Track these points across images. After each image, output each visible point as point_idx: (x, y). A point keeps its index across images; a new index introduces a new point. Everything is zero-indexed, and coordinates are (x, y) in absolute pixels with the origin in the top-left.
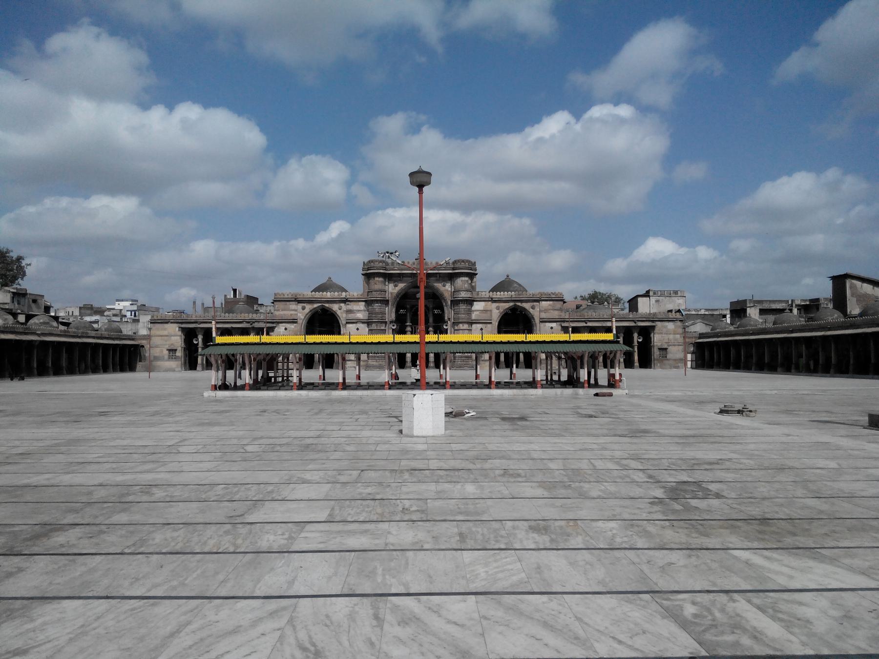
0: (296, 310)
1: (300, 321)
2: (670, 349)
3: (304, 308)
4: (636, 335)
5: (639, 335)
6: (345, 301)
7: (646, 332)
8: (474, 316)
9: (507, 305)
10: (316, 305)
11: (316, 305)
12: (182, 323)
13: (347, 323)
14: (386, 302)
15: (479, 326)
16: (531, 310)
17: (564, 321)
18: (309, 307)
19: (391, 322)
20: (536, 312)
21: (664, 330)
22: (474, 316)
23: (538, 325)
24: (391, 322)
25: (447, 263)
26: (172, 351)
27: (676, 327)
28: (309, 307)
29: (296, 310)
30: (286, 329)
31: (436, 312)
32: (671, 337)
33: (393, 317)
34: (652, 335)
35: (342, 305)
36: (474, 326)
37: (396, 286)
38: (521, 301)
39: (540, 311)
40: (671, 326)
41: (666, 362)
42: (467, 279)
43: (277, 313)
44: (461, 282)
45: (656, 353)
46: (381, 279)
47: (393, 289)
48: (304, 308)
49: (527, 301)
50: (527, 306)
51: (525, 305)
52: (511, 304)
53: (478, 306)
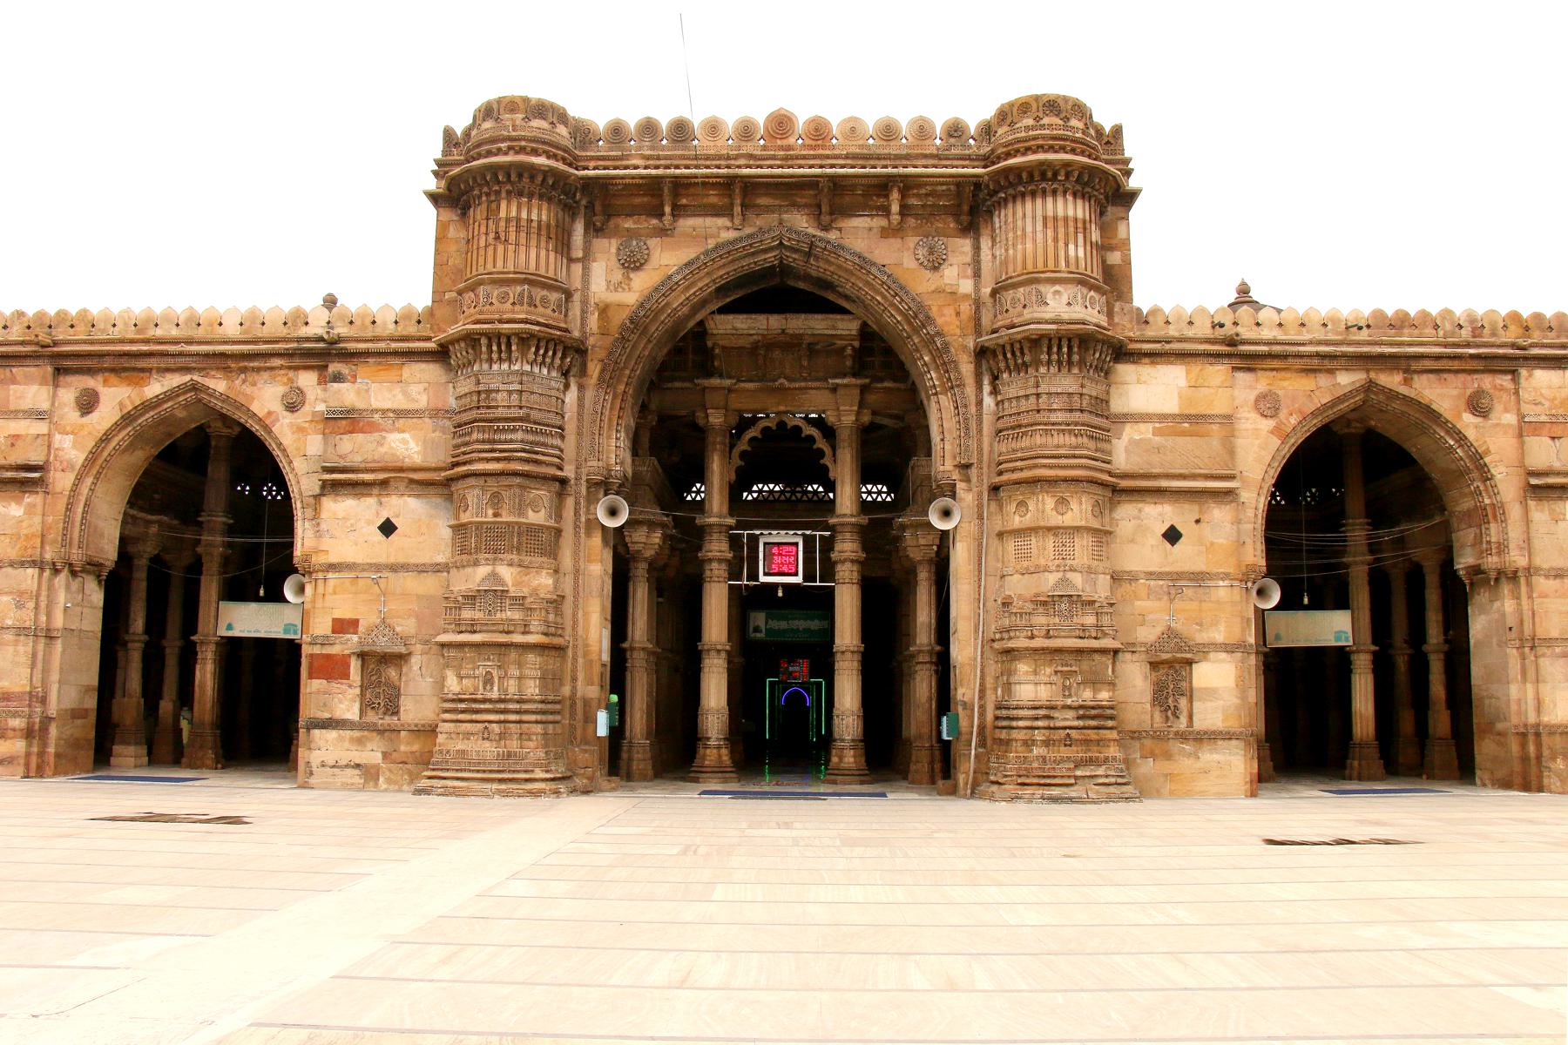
0: (39, 415)
1: (62, 481)
3: (88, 404)
8: (1125, 452)
10: (155, 387)
11: (155, 387)
13: (332, 487)
14: (566, 352)
15: (1159, 515)
16: (1468, 423)
18: (115, 398)
19: (602, 485)
23: (1515, 512)
24: (602, 485)
25: (955, 130)
28: (115, 398)
29: (39, 415)
31: (878, 492)
33: (614, 452)
35: (307, 380)
36: (1127, 514)
37: (633, 264)
39: (1525, 428)
44: (1035, 229)
46: (540, 213)
47: (618, 282)
48: (88, 404)
50: (1443, 395)
52: (1347, 380)
53: (1149, 390)
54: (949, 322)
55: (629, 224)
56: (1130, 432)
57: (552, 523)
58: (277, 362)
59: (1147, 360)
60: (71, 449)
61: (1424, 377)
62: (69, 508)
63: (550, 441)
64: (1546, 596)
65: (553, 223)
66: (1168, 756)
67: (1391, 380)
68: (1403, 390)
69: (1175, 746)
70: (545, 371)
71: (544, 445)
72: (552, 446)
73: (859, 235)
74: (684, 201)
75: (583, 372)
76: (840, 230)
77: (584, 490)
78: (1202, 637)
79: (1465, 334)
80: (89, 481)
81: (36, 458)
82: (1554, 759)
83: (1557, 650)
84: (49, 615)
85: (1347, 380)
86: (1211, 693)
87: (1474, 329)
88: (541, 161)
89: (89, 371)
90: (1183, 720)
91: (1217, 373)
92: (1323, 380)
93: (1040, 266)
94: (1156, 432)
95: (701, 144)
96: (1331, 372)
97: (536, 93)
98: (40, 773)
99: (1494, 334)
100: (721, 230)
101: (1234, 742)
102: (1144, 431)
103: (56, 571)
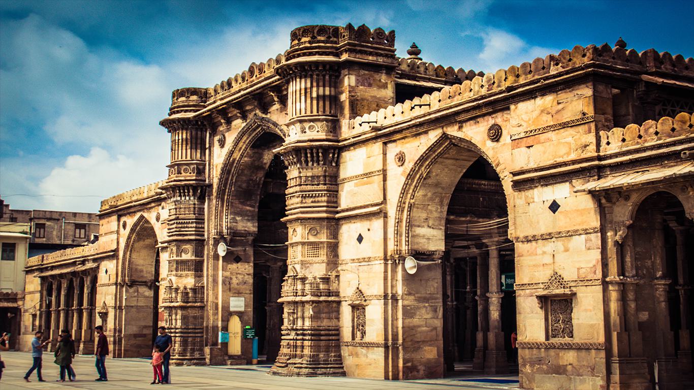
12: (41, 270)
17: (599, 172)
26: (34, 316)
30: (106, 272)
48: (124, 226)
50: (475, 133)
52: (434, 136)
55: (221, 129)
57: (193, 258)
58: (153, 205)
59: (352, 148)
61: (468, 123)
62: (123, 263)
63: (190, 225)
64: (522, 256)
65: (189, 137)
66: (357, 355)
67: (453, 131)
68: (459, 134)
69: (360, 350)
70: (187, 198)
71: (187, 227)
72: (191, 227)
74: (230, 115)
75: (211, 194)
76: (270, 113)
77: (211, 242)
79: (484, 91)
80: (129, 253)
81: (114, 247)
82: (524, 365)
83: (528, 291)
84: (121, 301)
85: (434, 136)
86: (372, 321)
87: (489, 86)
89: (125, 215)
90: (367, 339)
92: (423, 137)
93: (303, 114)
94: (356, 185)
96: (426, 132)
98: (119, 356)
99: (499, 86)
101: (380, 349)
103: (123, 286)
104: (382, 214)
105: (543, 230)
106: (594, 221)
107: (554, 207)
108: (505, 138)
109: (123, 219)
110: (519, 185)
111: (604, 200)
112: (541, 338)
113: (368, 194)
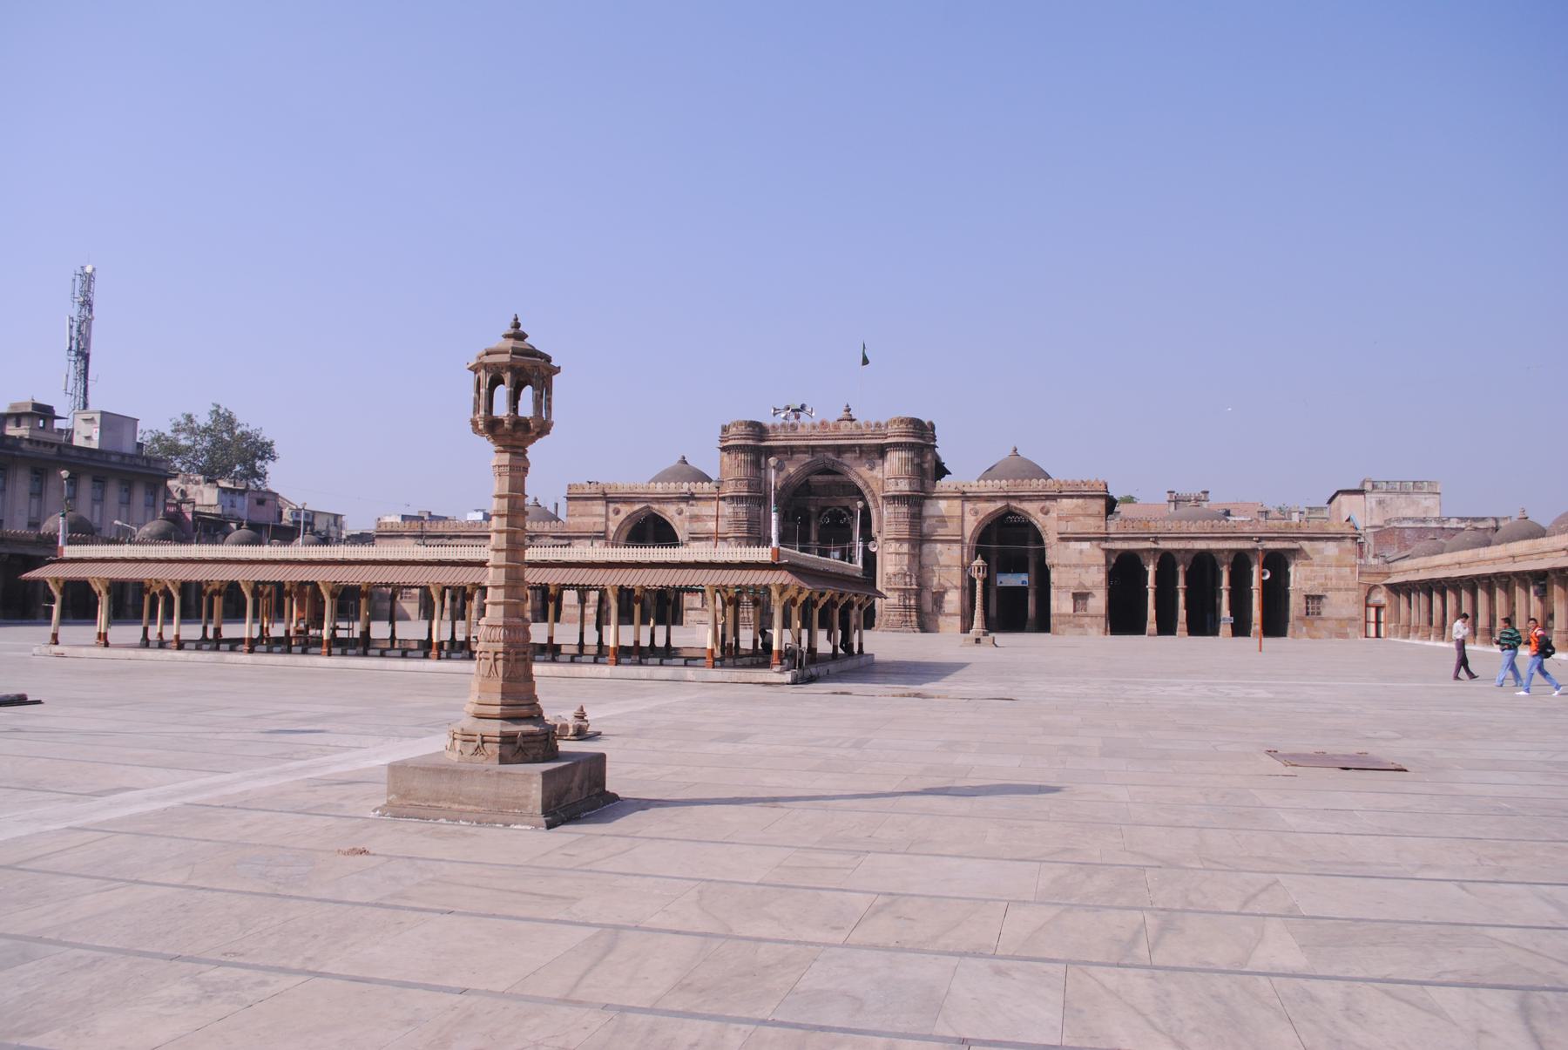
2: (1328, 594)
4: (1256, 570)
5: (1265, 565)
6: (690, 498)
7: (1277, 563)
9: (992, 507)
10: (637, 507)
17: (1106, 540)
18: (626, 510)
20: (1049, 521)
21: (1316, 558)
22: (925, 530)
25: (878, 425)
27: (1341, 551)
28: (626, 510)
32: (1332, 572)
34: (1292, 569)
35: (683, 506)
38: (1021, 499)
39: (1060, 518)
40: (1331, 549)
41: (1318, 623)
42: (910, 455)
43: (572, 521)
45: (1296, 604)
48: (617, 512)
49: (1030, 499)
50: (1032, 508)
51: (1026, 506)
52: (1000, 504)
54: (874, 486)
56: (928, 522)
60: (613, 528)
67: (1014, 504)
73: (848, 458)
78: (948, 585)
81: (602, 528)
88: (750, 442)
91: (957, 503)
95: (800, 431)
97: (749, 419)
100: (807, 458)
102: (933, 521)
104: (961, 542)
105: (1074, 561)
106: (1103, 561)
107: (1081, 552)
108: (1053, 514)
109: (612, 506)
110: (1063, 539)
111: (1108, 552)
112: (1071, 611)
113: (952, 529)
